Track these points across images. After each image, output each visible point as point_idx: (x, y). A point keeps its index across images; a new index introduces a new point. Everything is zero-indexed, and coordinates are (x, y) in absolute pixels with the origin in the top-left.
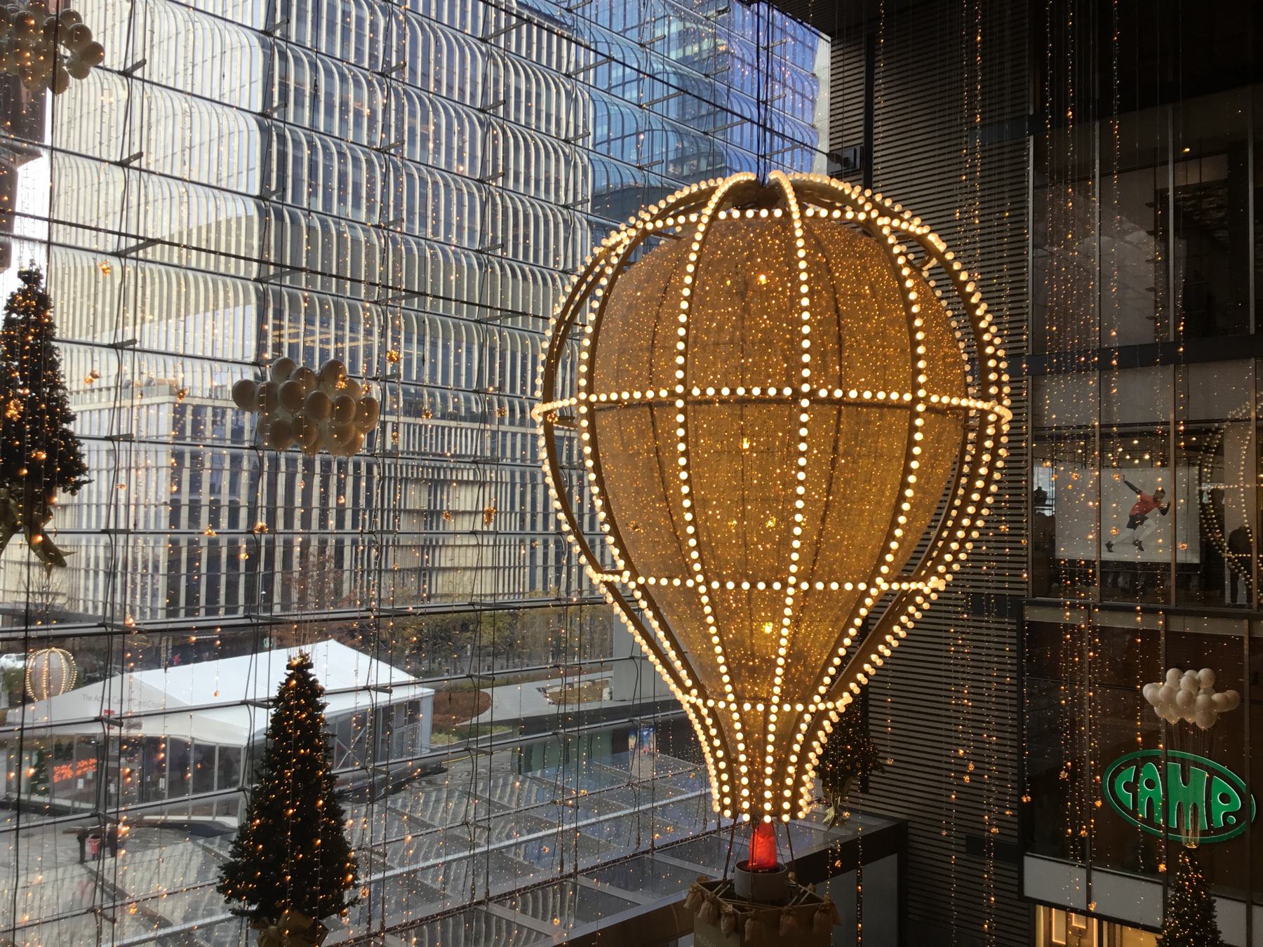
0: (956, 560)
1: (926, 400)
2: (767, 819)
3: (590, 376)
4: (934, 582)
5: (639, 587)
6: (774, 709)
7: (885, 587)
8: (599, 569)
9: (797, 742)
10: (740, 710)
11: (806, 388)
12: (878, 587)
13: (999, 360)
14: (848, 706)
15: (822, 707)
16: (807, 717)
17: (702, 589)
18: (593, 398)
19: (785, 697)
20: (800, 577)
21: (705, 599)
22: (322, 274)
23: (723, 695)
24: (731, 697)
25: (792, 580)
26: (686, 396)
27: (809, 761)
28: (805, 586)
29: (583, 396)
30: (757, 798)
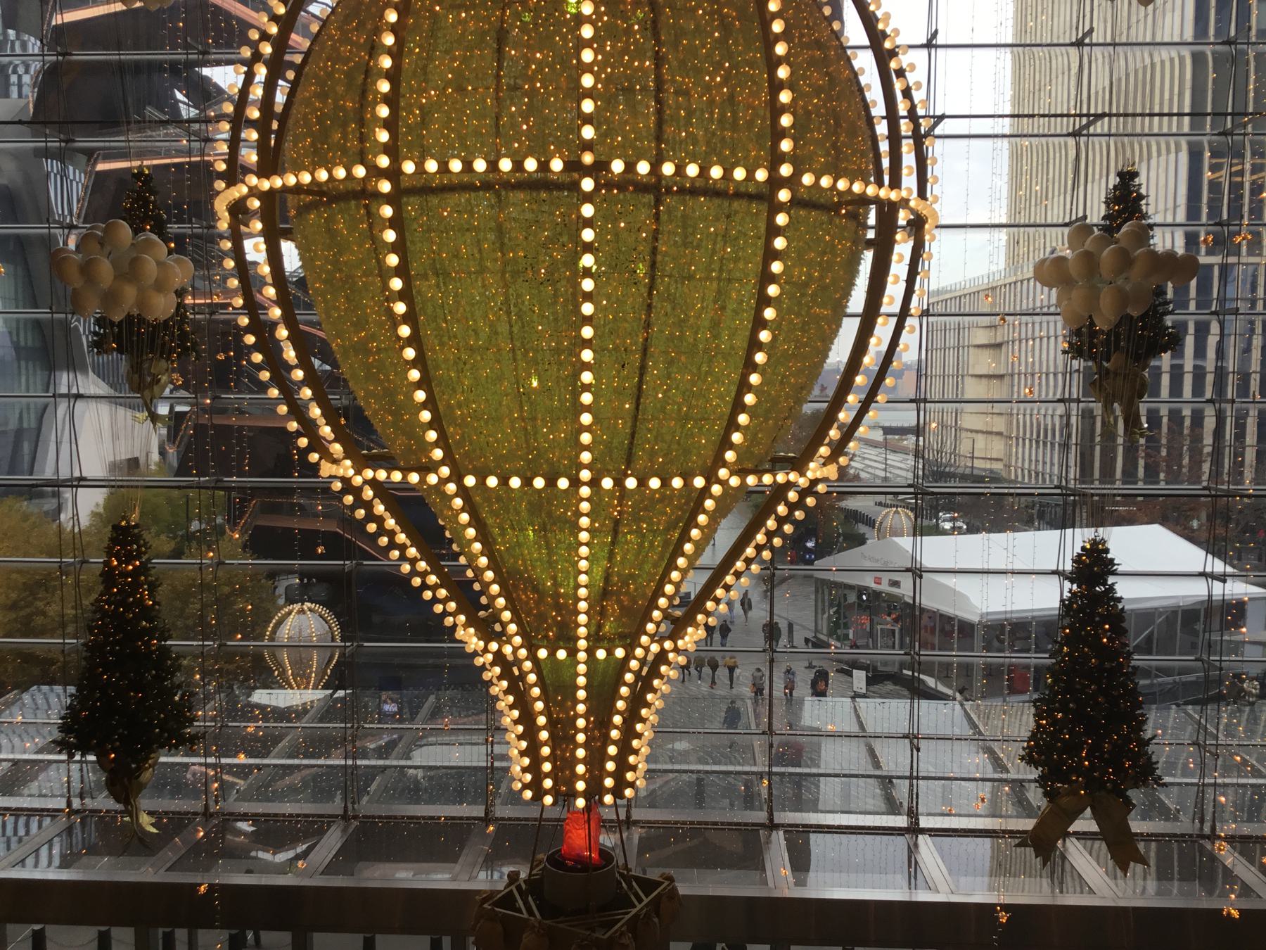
6: (582, 656)
7: (735, 481)
10: (532, 656)
11: (588, 158)
12: (724, 483)
13: (254, 46)
17: (451, 488)
19: (595, 639)
21: (458, 502)
24: (518, 640)
25: (585, 475)
26: (393, 173)
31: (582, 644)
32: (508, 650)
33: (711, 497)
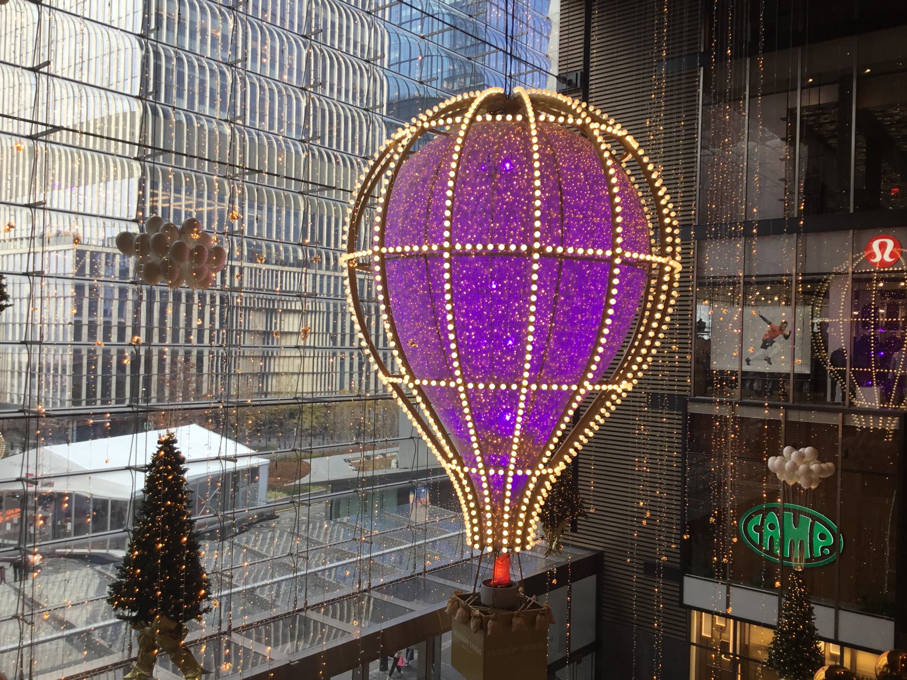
0: (640, 369)
1: (621, 256)
2: (505, 550)
3: (381, 234)
4: (625, 385)
5: (416, 387)
6: (511, 473)
7: (590, 388)
8: (386, 374)
9: (527, 497)
10: (487, 474)
11: (537, 245)
13: (674, 227)
14: (562, 471)
15: (544, 472)
16: (534, 479)
17: (461, 389)
18: (384, 250)
20: (531, 380)
21: (463, 396)
22: (278, 176)
23: (474, 464)
24: (480, 465)
27: (535, 510)
28: (534, 387)
29: (376, 248)
30: (498, 535)
31: (512, 467)
32: (474, 470)
33: (580, 394)
